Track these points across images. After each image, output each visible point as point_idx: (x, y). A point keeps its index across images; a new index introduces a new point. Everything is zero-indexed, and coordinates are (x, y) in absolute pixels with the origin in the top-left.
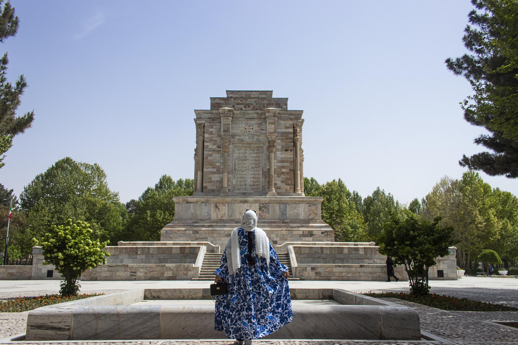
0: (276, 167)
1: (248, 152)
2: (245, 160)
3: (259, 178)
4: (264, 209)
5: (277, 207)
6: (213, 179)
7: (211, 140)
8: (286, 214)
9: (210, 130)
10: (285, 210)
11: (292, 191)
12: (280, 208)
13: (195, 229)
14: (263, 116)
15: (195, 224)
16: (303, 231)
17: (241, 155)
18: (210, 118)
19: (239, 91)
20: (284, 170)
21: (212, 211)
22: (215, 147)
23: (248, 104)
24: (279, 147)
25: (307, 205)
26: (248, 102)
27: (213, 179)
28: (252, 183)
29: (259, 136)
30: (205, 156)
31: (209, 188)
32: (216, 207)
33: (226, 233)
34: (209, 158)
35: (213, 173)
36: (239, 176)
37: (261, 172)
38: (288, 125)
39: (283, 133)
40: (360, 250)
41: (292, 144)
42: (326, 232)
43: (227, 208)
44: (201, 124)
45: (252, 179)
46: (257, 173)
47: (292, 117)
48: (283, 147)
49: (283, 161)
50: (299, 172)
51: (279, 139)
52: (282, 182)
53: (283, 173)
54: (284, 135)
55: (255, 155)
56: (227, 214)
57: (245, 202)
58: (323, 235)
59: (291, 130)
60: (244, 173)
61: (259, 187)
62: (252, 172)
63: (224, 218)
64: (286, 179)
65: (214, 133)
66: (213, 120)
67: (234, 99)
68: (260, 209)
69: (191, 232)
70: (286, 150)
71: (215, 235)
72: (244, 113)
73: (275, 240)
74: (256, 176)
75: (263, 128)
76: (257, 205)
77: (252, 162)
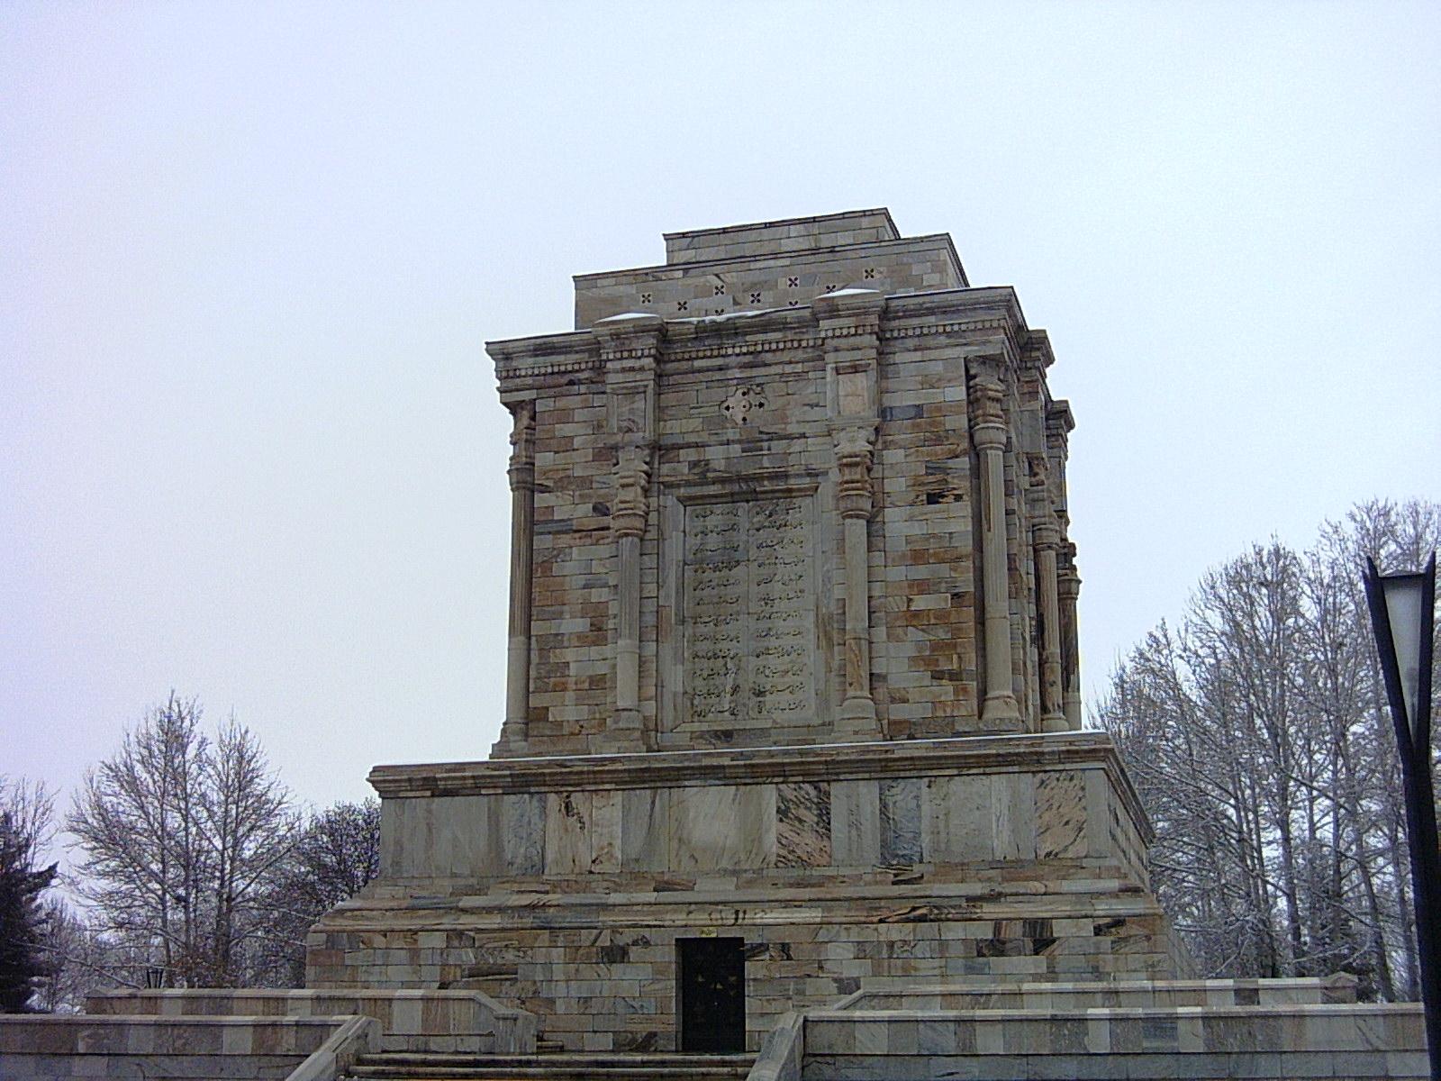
2: (732, 564)
4: (802, 812)
7: (564, 482)
14: (808, 338)
15: (466, 902)
16: (998, 924)
17: (713, 541)
19: (725, 231)
20: (920, 603)
23: (754, 285)
26: (751, 278)
33: (605, 941)
37: (809, 622)
40: (1182, 1026)
42: (1118, 922)
43: (617, 813)
48: (917, 483)
58: (1106, 941)
59: (960, 393)
61: (799, 695)
65: (577, 443)
67: (686, 271)
68: (783, 813)
69: (438, 941)
70: (933, 499)
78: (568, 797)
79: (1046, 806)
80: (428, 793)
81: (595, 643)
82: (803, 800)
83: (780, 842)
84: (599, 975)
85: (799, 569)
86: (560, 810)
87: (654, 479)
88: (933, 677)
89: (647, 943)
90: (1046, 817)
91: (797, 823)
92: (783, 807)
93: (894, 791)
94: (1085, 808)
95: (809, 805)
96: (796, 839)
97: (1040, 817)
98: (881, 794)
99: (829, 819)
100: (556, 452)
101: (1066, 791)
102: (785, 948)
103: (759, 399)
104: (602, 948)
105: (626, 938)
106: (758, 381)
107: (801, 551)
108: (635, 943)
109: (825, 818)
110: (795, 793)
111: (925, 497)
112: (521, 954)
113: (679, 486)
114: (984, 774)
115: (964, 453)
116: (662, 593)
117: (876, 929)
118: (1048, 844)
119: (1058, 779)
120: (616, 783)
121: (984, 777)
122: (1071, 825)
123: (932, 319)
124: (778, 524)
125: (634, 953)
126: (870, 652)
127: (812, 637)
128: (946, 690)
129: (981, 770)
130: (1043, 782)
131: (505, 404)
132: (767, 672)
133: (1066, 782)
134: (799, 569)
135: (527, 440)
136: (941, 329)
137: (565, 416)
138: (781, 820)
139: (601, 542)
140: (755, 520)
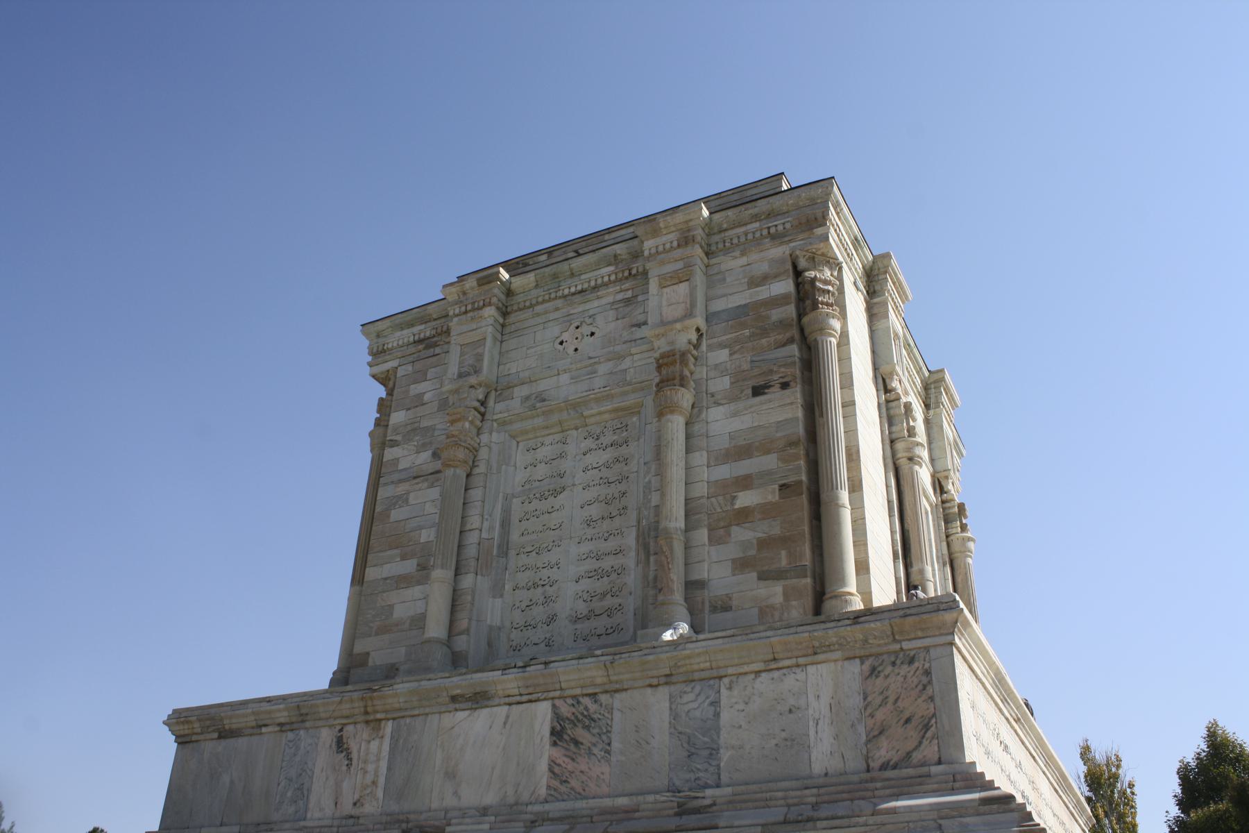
0: (701, 490)
1: (571, 449)
2: (556, 493)
3: (620, 571)
4: (580, 733)
5: (657, 706)
6: (400, 612)
8: (714, 751)
9: (416, 389)
10: (712, 726)
11: (799, 609)
12: (675, 716)
17: (542, 471)
18: (420, 341)
20: (746, 499)
21: (317, 771)
24: (722, 384)
25: (855, 668)
28: (582, 608)
29: (620, 357)
30: (378, 509)
31: (376, 659)
32: (340, 745)
34: (395, 515)
35: (403, 581)
36: (523, 578)
37: (631, 540)
39: (743, 310)
41: (794, 350)
45: (586, 584)
46: (611, 545)
47: (779, 224)
48: (738, 377)
49: (741, 452)
50: (844, 496)
51: (722, 346)
52: (741, 565)
53: (743, 516)
54: (750, 317)
55: (606, 456)
57: (479, 699)
59: (785, 286)
62: (585, 548)
63: (369, 808)
64: (763, 544)
65: (427, 397)
66: (427, 347)
70: (758, 391)
72: (555, 276)
74: (607, 563)
75: (641, 318)
76: (544, 708)
77: (590, 494)
78: (341, 730)
79: (878, 700)
81: (419, 583)
82: (580, 717)
85: (622, 487)
87: (487, 417)
88: (760, 578)
90: (880, 715)
91: (572, 747)
92: (558, 728)
93: (686, 698)
94: (932, 698)
95: (587, 723)
97: (872, 716)
98: (671, 703)
99: (609, 738)
101: (905, 677)
103: (586, 330)
106: (591, 312)
107: (626, 468)
109: (604, 737)
110: (574, 710)
111: (750, 391)
113: (511, 423)
114: (798, 666)
115: (791, 341)
116: (486, 524)
118: (883, 752)
119: (894, 664)
120: (386, 712)
121: (798, 670)
122: (914, 722)
123: (757, 225)
126: (686, 558)
127: (633, 554)
128: (775, 592)
129: (793, 661)
130: (873, 669)
131: (373, 376)
132: (585, 596)
133: (905, 667)
134: (622, 487)
135: (384, 407)
136: (765, 232)
137: (421, 376)
138: (555, 744)
140: (583, 445)
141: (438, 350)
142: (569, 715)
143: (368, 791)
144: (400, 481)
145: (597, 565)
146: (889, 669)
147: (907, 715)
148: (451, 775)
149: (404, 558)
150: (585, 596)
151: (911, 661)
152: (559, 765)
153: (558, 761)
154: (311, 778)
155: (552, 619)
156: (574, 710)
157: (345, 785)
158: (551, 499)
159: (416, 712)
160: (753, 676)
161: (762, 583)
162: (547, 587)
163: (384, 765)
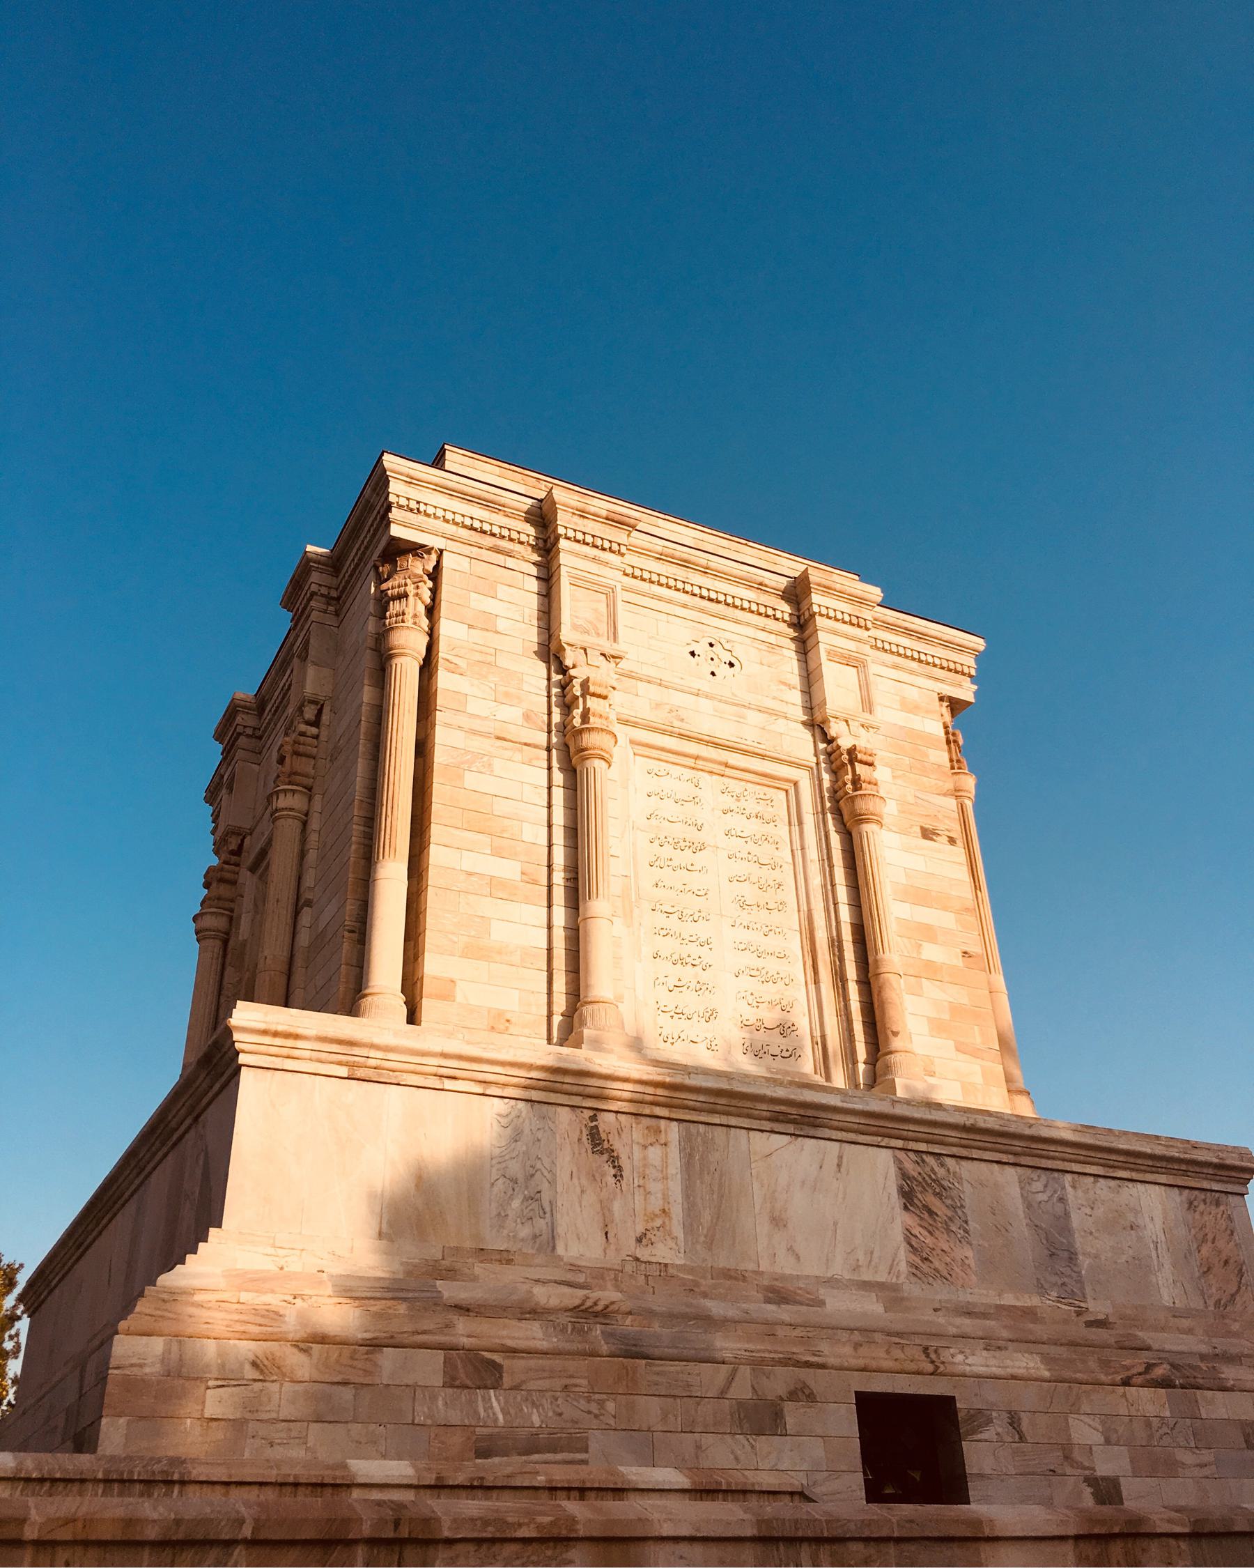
8: (1072, 1257)
9: (480, 603)
10: (1063, 1222)
13: (464, 1331)
15: (450, 1291)
17: (669, 809)
20: (932, 952)
21: (563, 1176)
22: (511, 714)
27: (499, 933)
33: (742, 1390)
34: (470, 780)
35: (495, 887)
37: (794, 945)
38: (912, 694)
44: (416, 549)
45: (746, 983)
52: (938, 1028)
56: (677, 1211)
60: (688, 929)
63: (663, 1252)
64: (956, 1010)
65: (502, 625)
68: (907, 1197)
70: (927, 834)
71: (650, 1409)
73: (1104, 1469)
74: (772, 965)
77: (741, 868)
78: (593, 1118)
80: (344, 1071)
83: (912, 1246)
84: (737, 1459)
86: (579, 1140)
89: (811, 1398)
90: (1205, 1250)
91: (926, 1216)
96: (929, 1240)
100: (471, 627)
102: (1014, 1420)
103: (727, 657)
104: (741, 1404)
105: (778, 1383)
107: (777, 853)
108: (793, 1396)
112: (594, 1408)
117: (1124, 1395)
122: (1232, 1266)
124: (747, 812)
125: (793, 1415)
132: (750, 999)
133: (1213, 1207)
139: (535, 762)
141: (510, 562)
142: (916, 1175)
143: (658, 1223)
144: (473, 732)
145: (759, 963)
146: (1202, 1207)
147: (1224, 1257)
148: (778, 1222)
149: (497, 853)
150: (750, 999)
151: (1218, 1204)
152: (916, 1236)
153: (915, 1232)
154: (552, 1183)
155: (711, 1015)
156: (919, 1169)
157: (617, 1206)
158: (688, 852)
159: (716, 1119)
160: (1092, 1179)
161: (961, 1056)
162: (698, 969)
163: (676, 1188)
